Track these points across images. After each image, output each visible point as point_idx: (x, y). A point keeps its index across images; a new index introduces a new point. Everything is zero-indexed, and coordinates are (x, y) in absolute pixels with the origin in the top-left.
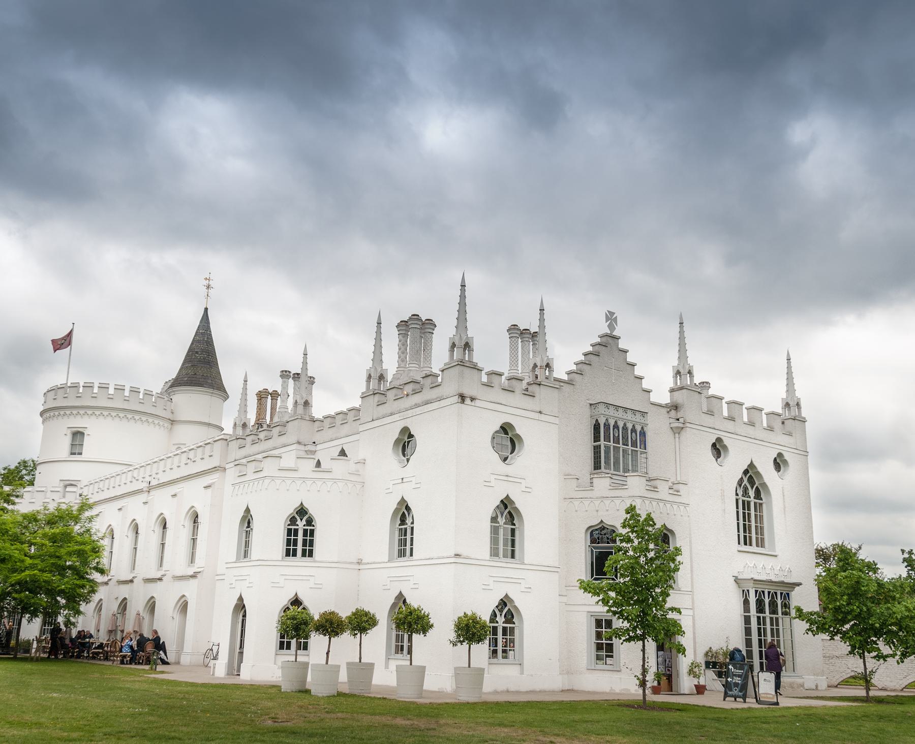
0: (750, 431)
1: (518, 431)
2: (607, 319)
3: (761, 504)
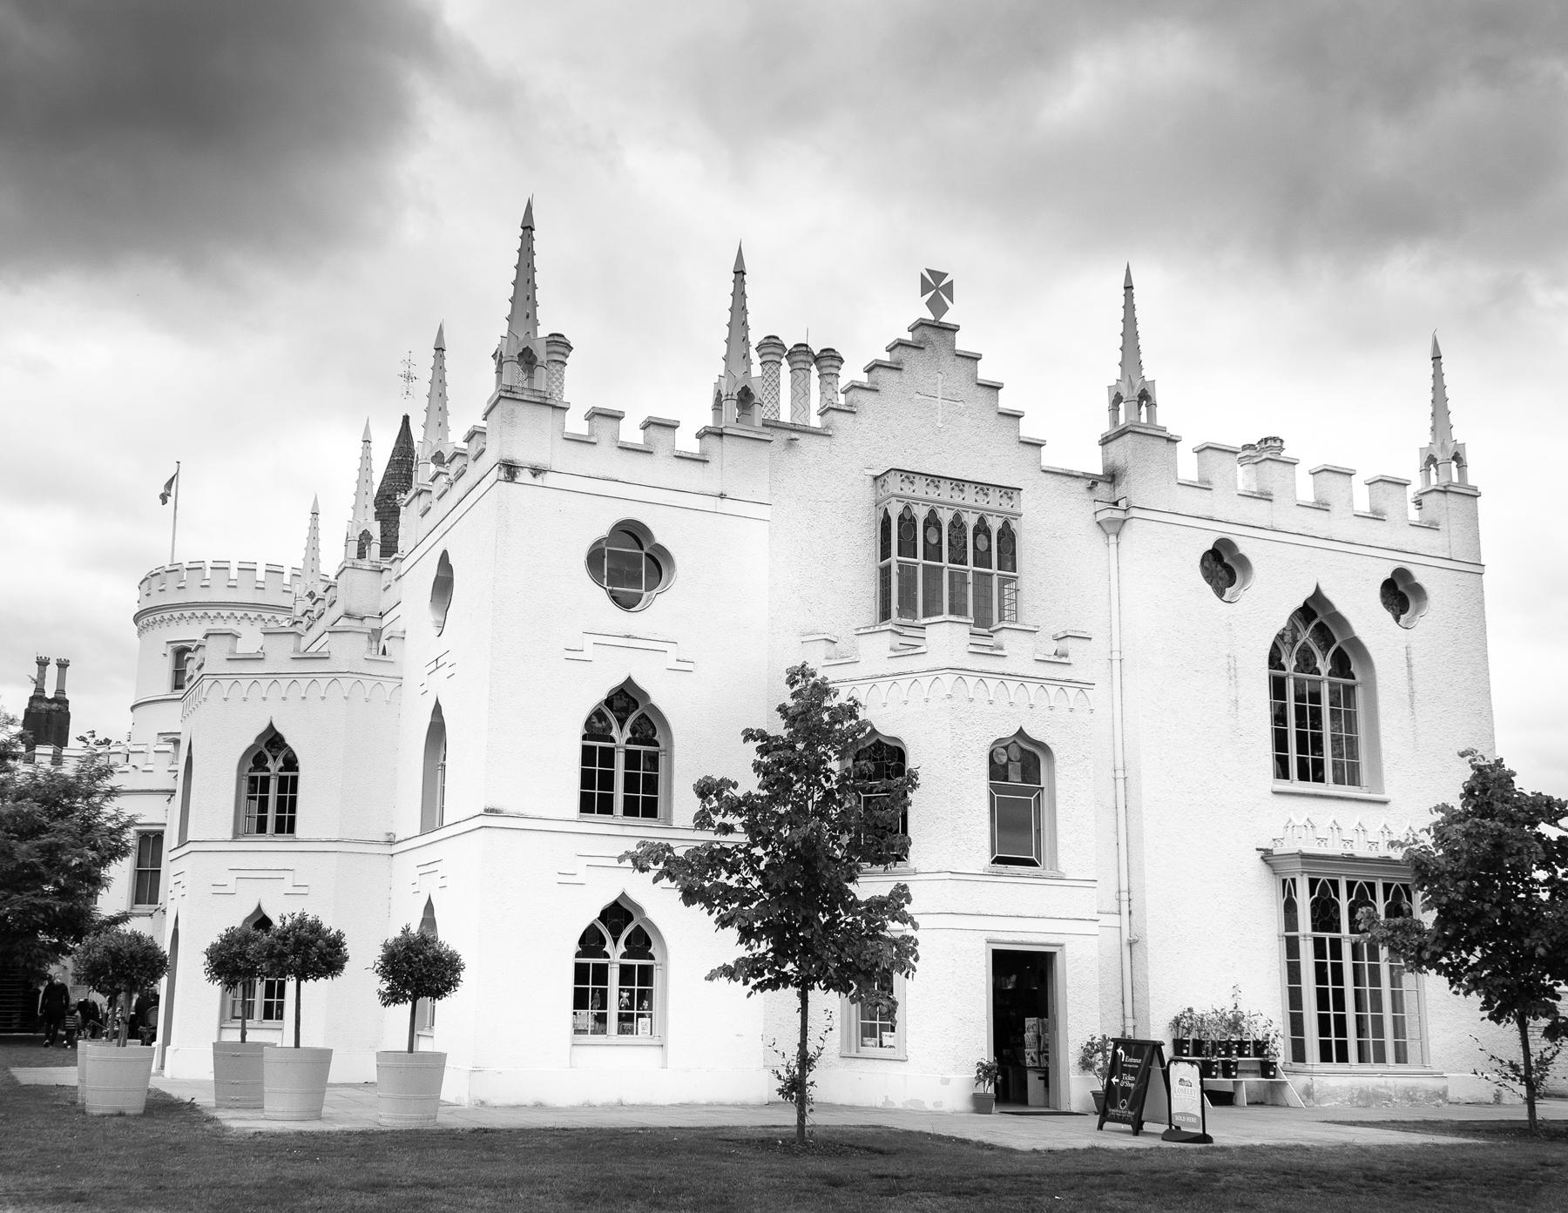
0: (1316, 522)
1: (659, 538)
2: (926, 286)
3: (1350, 689)
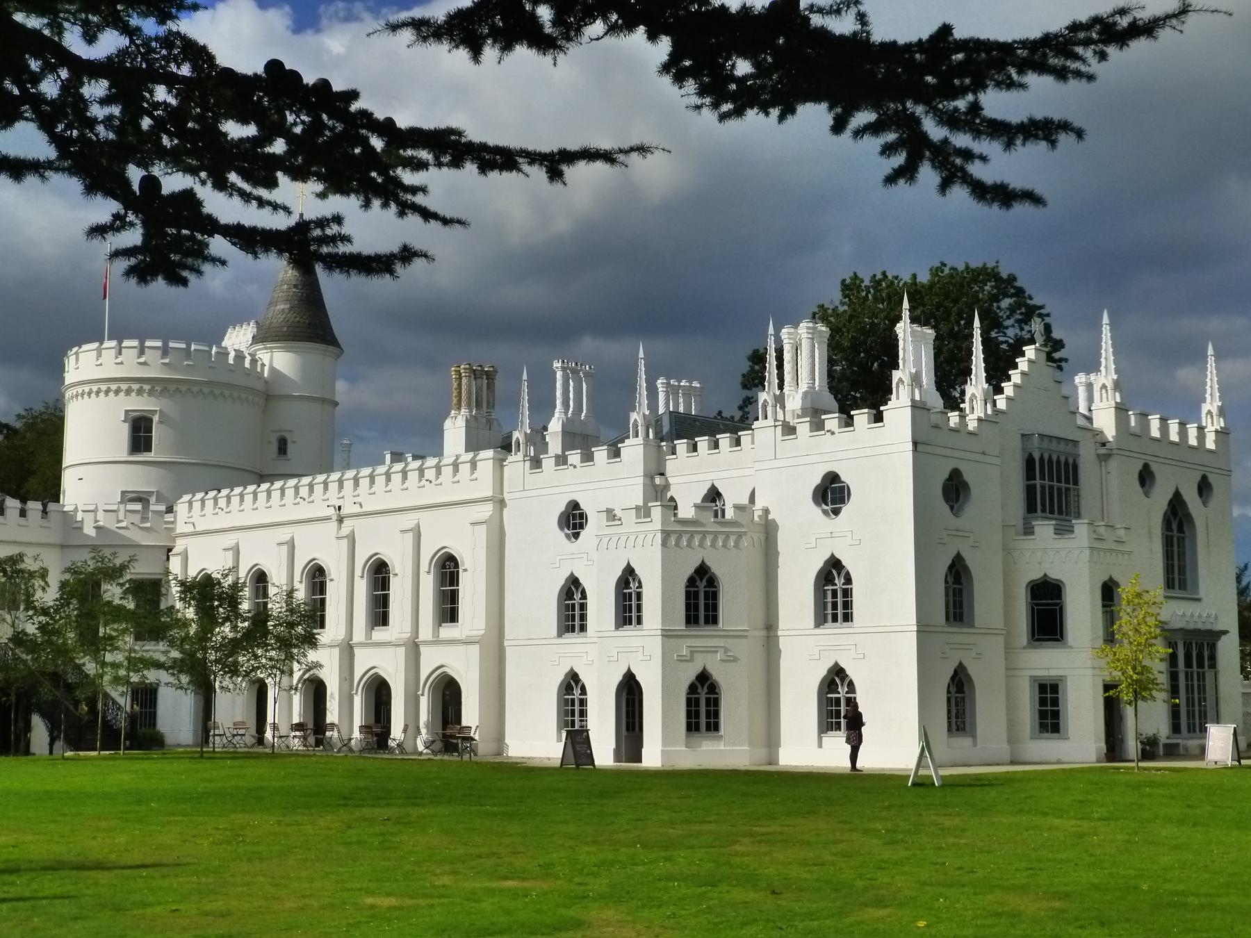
3: (1183, 539)
